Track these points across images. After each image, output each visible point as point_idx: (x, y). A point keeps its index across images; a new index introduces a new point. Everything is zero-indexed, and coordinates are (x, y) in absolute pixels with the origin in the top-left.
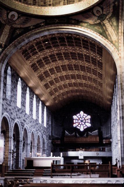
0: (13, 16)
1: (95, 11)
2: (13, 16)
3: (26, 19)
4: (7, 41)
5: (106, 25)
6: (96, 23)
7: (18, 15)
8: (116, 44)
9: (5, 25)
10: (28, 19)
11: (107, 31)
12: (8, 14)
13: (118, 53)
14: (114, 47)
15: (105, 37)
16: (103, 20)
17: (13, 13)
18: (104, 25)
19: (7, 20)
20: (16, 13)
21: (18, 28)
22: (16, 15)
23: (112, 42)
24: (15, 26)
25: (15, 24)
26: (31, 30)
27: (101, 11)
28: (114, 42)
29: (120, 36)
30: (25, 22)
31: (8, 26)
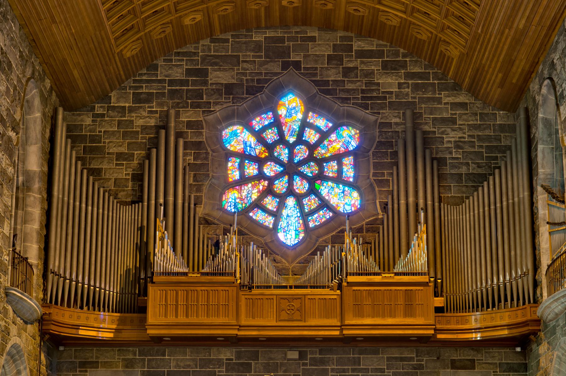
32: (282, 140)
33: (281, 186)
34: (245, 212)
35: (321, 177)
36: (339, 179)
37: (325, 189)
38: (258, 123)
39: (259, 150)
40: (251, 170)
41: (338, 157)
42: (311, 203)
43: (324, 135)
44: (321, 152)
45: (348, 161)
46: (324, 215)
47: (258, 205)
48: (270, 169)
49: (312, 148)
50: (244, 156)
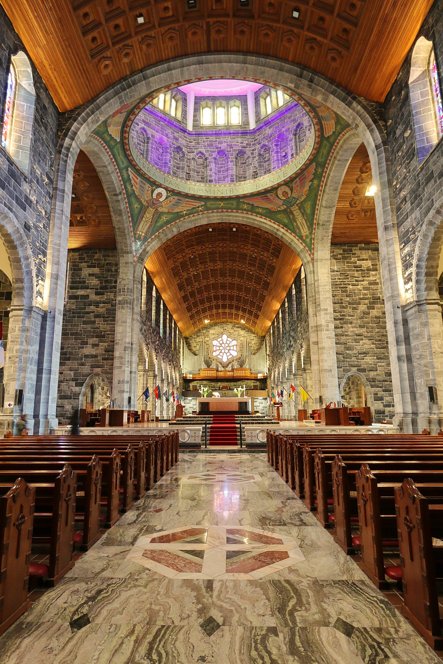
0: (160, 195)
1: (280, 192)
2: (160, 195)
3: (178, 199)
4: (147, 232)
5: (294, 212)
6: (279, 209)
7: (167, 193)
8: (308, 240)
9: (148, 207)
10: (180, 200)
11: (296, 222)
12: (153, 192)
13: (309, 252)
14: (304, 244)
15: (290, 230)
16: (291, 206)
17: (160, 190)
18: (291, 213)
19: (150, 200)
20: (164, 190)
21: (165, 213)
22: (164, 192)
23: (301, 237)
24: (160, 209)
25: (162, 206)
26: (183, 216)
27: (289, 192)
28: (304, 238)
29: (315, 229)
30: (177, 204)
31: (151, 209)
32: (223, 343)
33: (223, 351)
34: (217, 356)
35: (230, 350)
36: (233, 350)
37: (231, 351)
38: (219, 340)
39: (219, 345)
40: (218, 348)
41: (233, 346)
42: (228, 354)
43: (231, 342)
44: (230, 345)
45: (235, 347)
46: (231, 356)
47: (219, 355)
48: (221, 348)
49: (229, 344)
50: (216, 346)
